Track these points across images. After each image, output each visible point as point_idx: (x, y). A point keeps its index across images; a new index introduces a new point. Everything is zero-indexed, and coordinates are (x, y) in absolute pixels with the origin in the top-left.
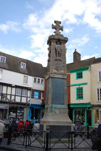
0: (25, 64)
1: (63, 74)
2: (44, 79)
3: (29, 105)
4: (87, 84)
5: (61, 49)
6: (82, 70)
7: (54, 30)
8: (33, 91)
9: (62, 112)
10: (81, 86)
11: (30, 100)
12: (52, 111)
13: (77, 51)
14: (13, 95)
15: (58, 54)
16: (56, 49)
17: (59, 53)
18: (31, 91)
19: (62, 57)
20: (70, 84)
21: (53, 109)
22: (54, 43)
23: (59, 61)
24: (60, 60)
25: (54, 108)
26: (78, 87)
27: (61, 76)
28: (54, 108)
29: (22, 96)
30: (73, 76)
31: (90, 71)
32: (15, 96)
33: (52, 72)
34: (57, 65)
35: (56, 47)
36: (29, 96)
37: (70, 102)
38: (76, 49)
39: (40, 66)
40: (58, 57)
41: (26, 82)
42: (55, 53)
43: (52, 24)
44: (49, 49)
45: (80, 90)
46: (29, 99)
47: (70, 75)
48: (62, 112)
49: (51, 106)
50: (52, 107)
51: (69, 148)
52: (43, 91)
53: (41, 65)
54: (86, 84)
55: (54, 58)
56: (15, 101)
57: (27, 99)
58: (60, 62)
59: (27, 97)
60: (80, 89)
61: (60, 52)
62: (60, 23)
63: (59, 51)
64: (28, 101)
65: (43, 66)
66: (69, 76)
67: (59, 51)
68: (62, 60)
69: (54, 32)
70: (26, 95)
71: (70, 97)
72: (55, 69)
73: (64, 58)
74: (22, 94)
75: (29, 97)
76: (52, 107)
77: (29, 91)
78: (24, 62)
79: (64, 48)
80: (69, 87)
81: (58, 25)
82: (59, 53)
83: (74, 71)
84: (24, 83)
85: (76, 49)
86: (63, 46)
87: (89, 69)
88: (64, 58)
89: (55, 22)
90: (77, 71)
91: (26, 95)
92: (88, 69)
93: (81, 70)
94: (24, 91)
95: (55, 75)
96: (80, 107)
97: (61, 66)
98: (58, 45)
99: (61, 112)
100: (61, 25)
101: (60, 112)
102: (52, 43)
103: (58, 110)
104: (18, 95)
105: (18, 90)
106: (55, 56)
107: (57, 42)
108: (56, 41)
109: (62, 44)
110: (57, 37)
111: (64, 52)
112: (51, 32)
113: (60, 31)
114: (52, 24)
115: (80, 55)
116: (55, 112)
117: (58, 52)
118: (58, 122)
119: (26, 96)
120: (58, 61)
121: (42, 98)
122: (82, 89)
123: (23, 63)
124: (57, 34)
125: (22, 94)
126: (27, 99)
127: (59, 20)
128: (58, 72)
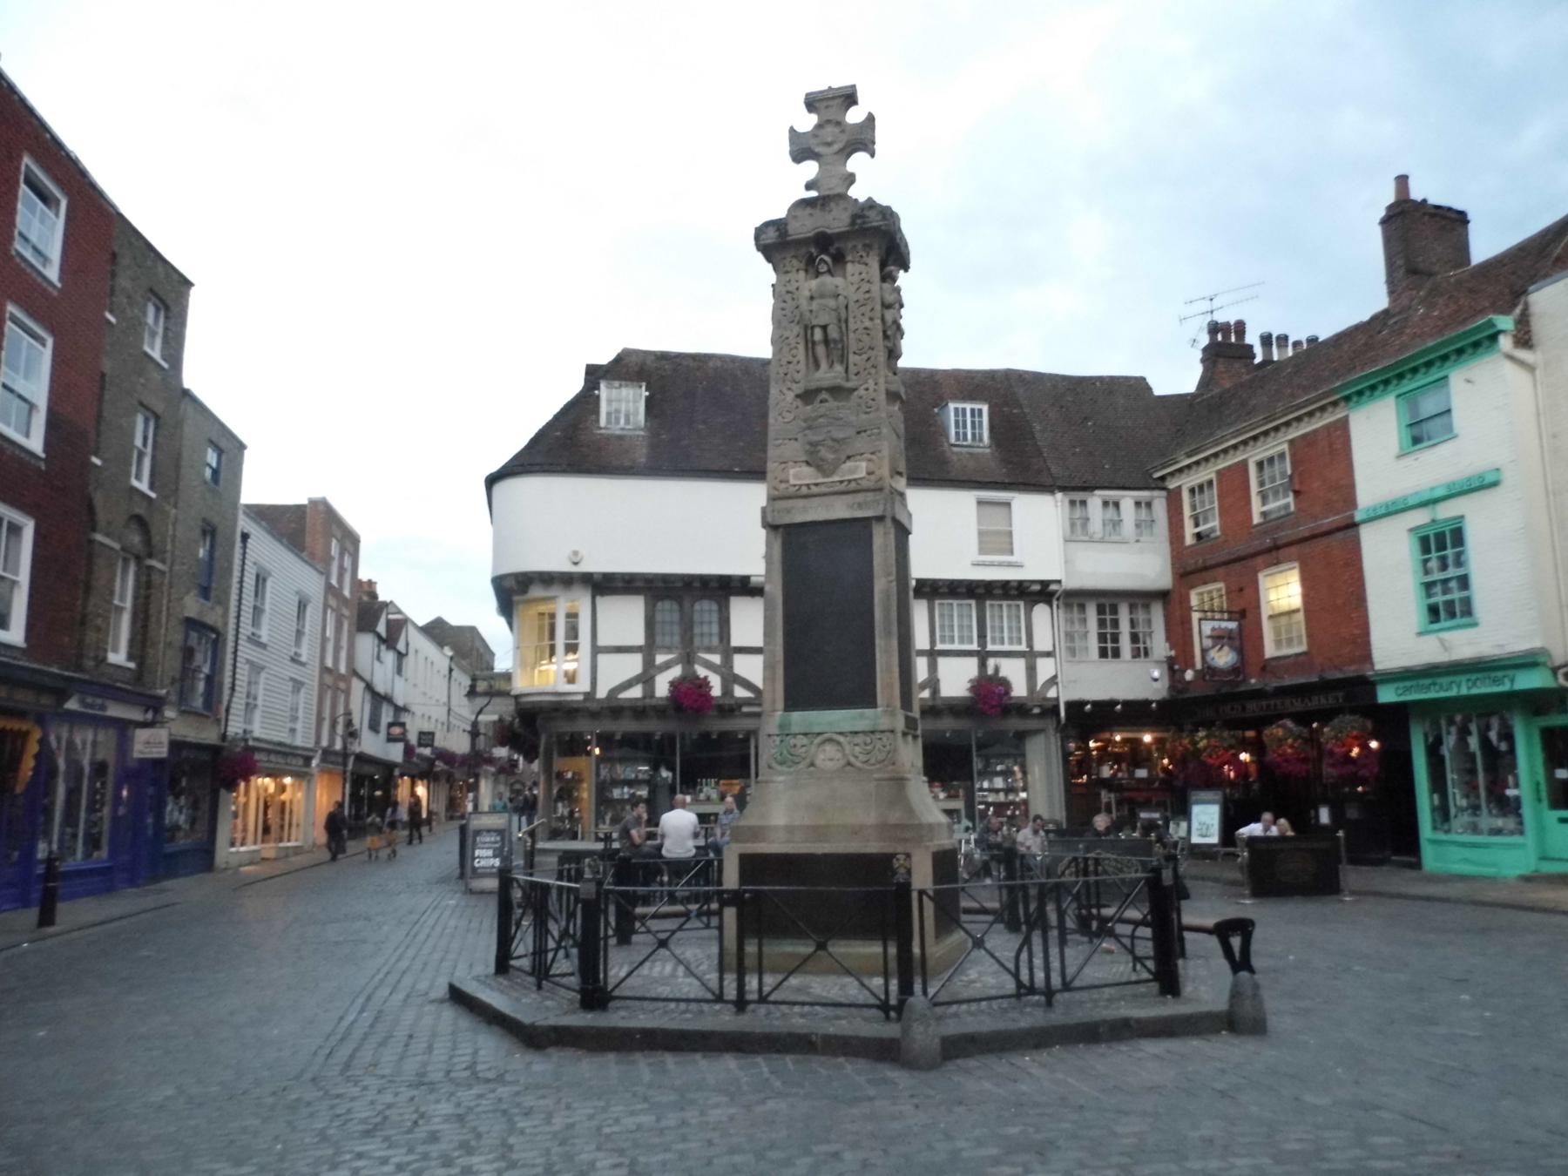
0: (985, 408)
1: (865, 484)
2: (1164, 493)
3: (1056, 709)
4: (1495, 484)
6: (1444, 358)
9: (863, 758)
10: (1446, 511)
12: (788, 760)
13: (1416, 193)
14: (921, 653)
15: (821, 350)
19: (852, 358)
20: (1350, 501)
21: (792, 741)
22: (793, 276)
23: (824, 395)
24: (837, 391)
25: (805, 734)
26: (1420, 518)
28: (805, 734)
29: (990, 647)
30: (1374, 429)
31: (1522, 354)
32: (933, 655)
33: (783, 486)
34: (809, 428)
35: (804, 303)
36: (1042, 642)
37: (1367, 657)
38: (1402, 181)
41: (997, 540)
43: (792, 130)
45: (1441, 546)
47: (1343, 425)
48: (863, 758)
49: (781, 726)
50: (785, 732)
51: (719, 998)
52: (1162, 595)
53: (1136, 387)
54: (1490, 479)
55: (794, 386)
56: (935, 691)
58: (832, 403)
59: (1031, 656)
60: (1440, 538)
61: (833, 333)
62: (849, 97)
63: (824, 328)
64: (1041, 679)
65: (1161, 388)
66: (1337, 443)
67: (824, 328)
68: (850, 385)
72: (808, 463)
73: (869, 365)
74: (982, 636)
76: (785, 732)
77: (1041, 613)
78: (971, 397)
79: (865, 287)
80: (1350, 532)
81: (829, 122)
82: (826, 341)
83: (1373, 388)
84: (982, 551)
85: (1402, 181)
86: (856, 278)
87: (1505, 342)
88: (869, 365)
89: (812, 103)
90: (1400, 377)
91: (1020, 643)
92: (1493, 338)
93: (1429, 364)
94: (1002, 615)
95: (800, 503)
96: (1453, 693)
97: (841, 435)
98: (814, 283)
99: (852, 760)
100: (854, 116)
101: (842, 762)
103: (830, 749)
104: (956, 646)
105: (997, 613)
108: (803, 251)
109: (849, 267)
110: (805, 227)
111: (868, 323)
113: (857, 162)
114: (792, 130)
115: (1454, 221)
116: (812, 764)
117: (818, 334)
118: (818, 832)
119: (1023, 647)
120: (820, 397)
121: (1160, 646)
122: (1458, 536)
123: (968, 406)
124: (824, 198)
125: (982, 636)
127: (839, 82)
128: (826, 474)
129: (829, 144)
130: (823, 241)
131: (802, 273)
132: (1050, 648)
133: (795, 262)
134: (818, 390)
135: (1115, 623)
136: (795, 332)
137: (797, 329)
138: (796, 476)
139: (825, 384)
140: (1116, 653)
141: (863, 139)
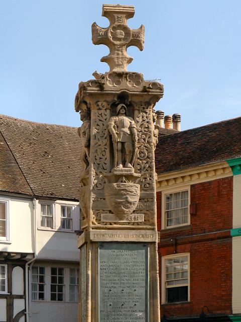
5: (132, 134)
7: (104, 50)
8: (39, 266)
11: (25, 310)
16: (111, 137)
17: (123, 150)
18: (27, 267)
22: (103, 111)
24: (129, 177)
27: (132, 236)
36: (18, 289)
39: (69, 141)
40: (121, 166)
42: (108, 151)
44: (84, 133)
46: (19, 305)
57: (10, 307)
61: (128, 147)
63: (123, 143)
68: (135, 175)
69: (104, 60)
70: (4, 290)
71: (231, 286)
72: (110, 212)
75: (20, 297)
77: (18, 272)
82: (123, 150)
97: (130, 199)
102: (94, 113)
106: (108, 161)
107: (114, 105)
112: (91, 63)
119: (6, 292)
120: (120, 180)
126: (10, 307)
129: (119, 39)
130: (123, 97)
131: (108, 111)
132: (22, 293)
133: (105, 104)
134: (121, 176)
135: (61, 280)
136: (104, 143)
137: (106, 141)
138: (104, 218)
139: (124, 173)
140: (60, 299)
141: (135, 41)
